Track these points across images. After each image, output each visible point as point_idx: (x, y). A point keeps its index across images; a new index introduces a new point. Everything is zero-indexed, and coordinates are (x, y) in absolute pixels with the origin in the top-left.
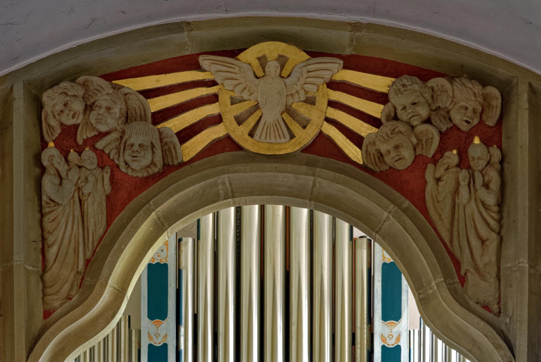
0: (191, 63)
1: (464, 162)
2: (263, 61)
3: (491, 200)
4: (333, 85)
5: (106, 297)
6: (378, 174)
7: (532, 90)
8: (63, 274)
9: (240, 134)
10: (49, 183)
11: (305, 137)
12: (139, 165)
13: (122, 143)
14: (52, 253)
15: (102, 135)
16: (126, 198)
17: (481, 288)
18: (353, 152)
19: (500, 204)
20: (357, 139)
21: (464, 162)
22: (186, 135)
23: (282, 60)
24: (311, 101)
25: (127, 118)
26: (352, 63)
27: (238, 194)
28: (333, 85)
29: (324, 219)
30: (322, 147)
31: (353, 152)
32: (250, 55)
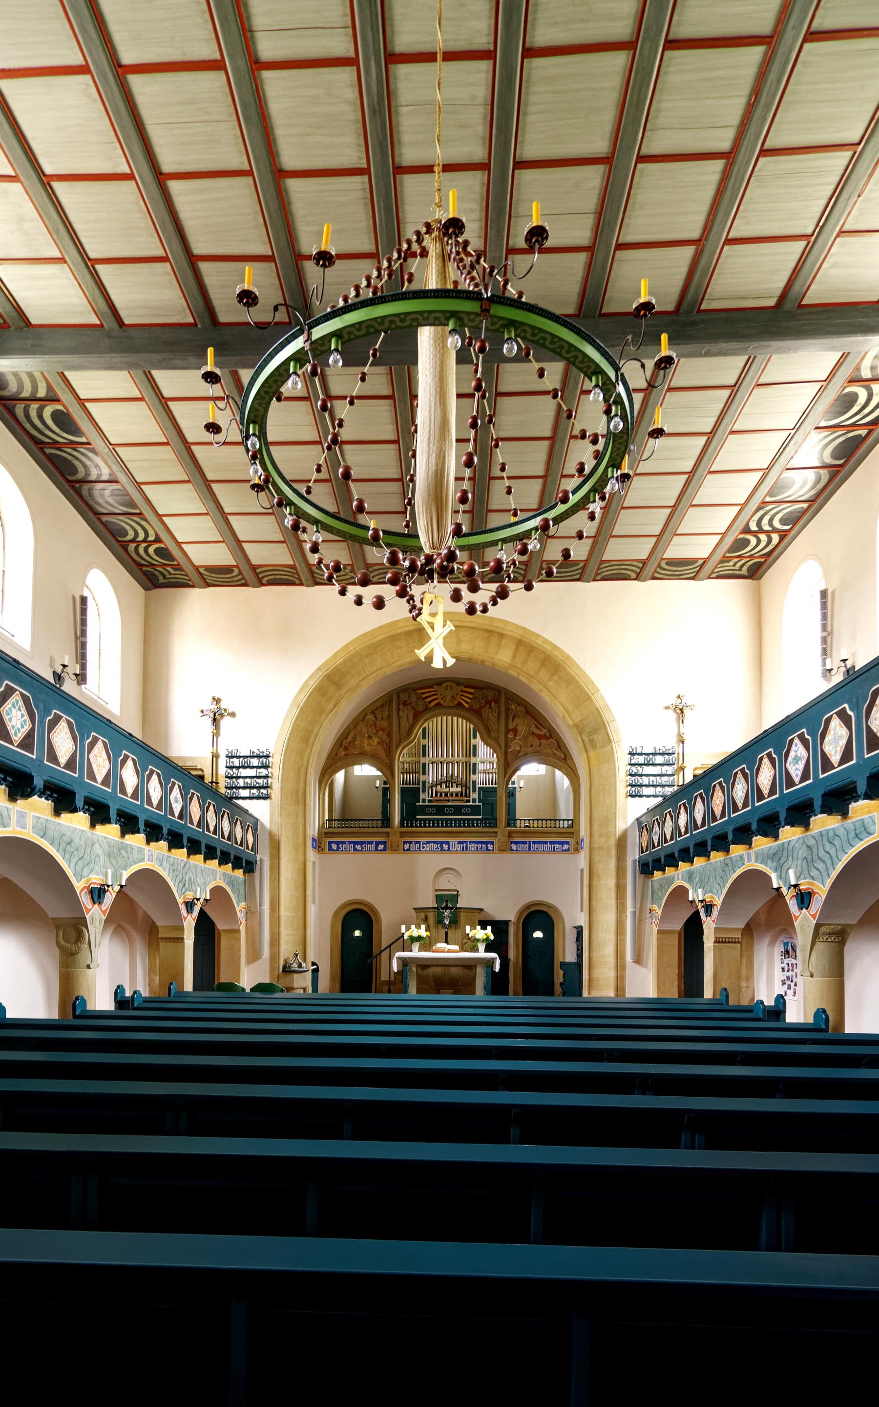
0: (431, 687)
1: (490, 707)
4: (462, 691)
6: (471, 710)
7: (506, 694)
8: (404, 731)
9: (442, 702)
10: (401, 713)
11: (456, 702)
12: (421, 708)
13: (417, 705)
16: (417, 716)
17: (494, 734)
18: (466, 705)
20: (467, 702)
21: (490, 707)
22: (430, 702)
25: (418, 698)
27: (442, 715)
28: (462, 691)
29: (460, 719)
30: (460, 704)
31: (466, 705)
32: (444, 685)
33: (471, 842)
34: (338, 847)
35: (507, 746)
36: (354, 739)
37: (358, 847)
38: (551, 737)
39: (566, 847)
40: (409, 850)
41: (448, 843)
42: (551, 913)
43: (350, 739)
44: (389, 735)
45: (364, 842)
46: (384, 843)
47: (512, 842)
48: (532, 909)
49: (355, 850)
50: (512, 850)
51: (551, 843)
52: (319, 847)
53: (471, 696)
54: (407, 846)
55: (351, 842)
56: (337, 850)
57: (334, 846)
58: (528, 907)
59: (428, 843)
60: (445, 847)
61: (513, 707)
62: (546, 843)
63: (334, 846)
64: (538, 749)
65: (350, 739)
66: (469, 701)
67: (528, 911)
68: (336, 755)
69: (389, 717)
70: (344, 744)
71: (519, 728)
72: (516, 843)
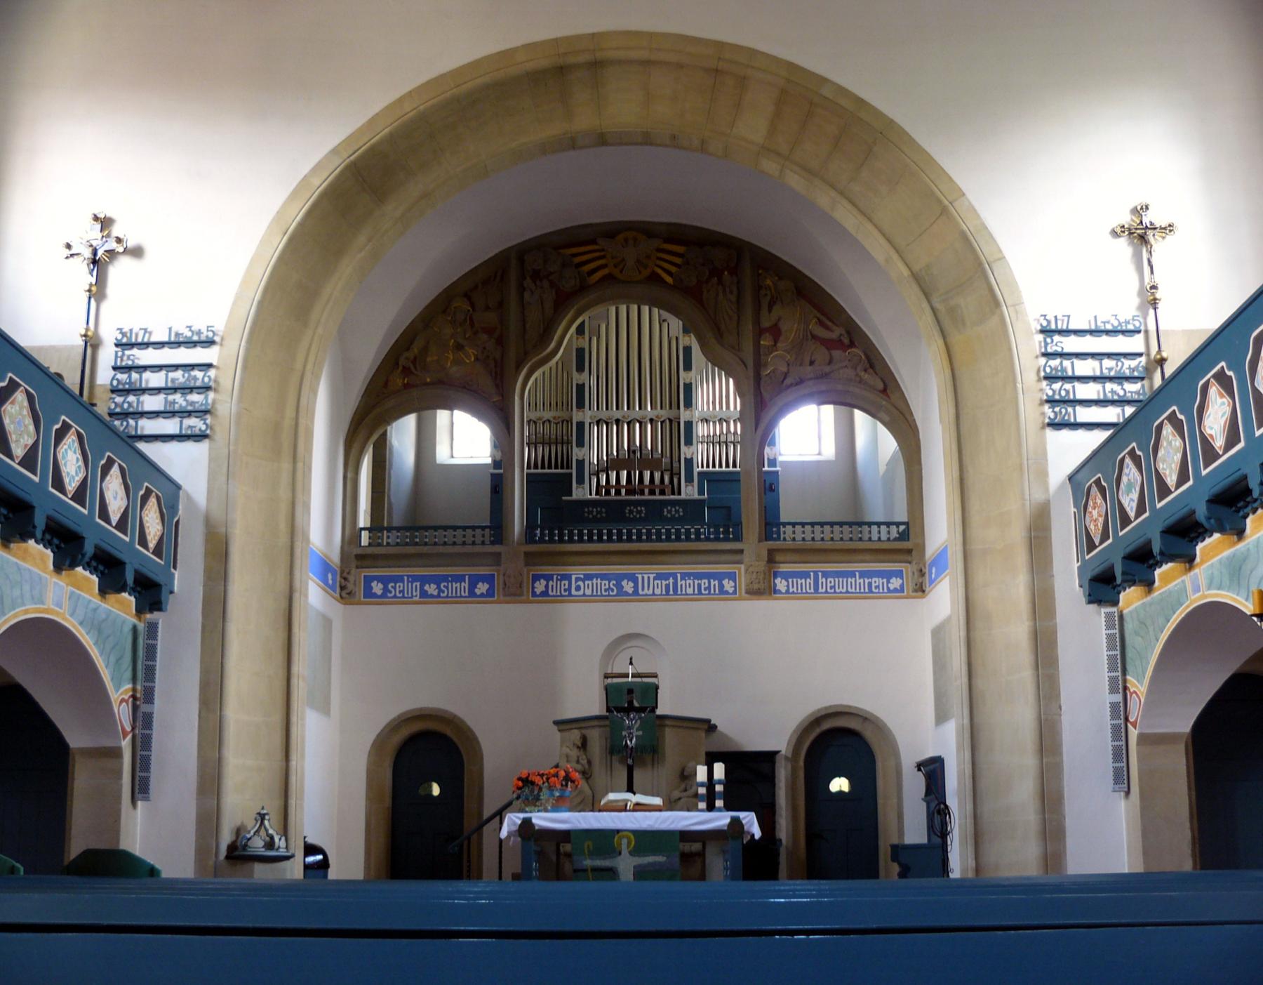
0: (594, 242)
1: (720, 282)
2: (626, 240)
3: (733, 298)
4: (659, 250)
5: (553, 345)
10: (527, 295)
11: (646, 273)
14: (528, 326)
15: (551, 273)
16: (563, 301)
18: (669, 280)
19: (738, 302)
21: (720, 282)
23: (635, 239)
24: (648, 257)
26: (668, 240)
28: (659, 250)
29: (656, 311)
31: (669, 280)
32: (620, 237)
33: (684, 576)
34: (386, 590)
35: (758, 366)
36: (425, 350)
37: (431, 589)
38: (852, 344)
39: (895, 583)
40: (545, 593)
41: (633, 578)
42: (869, 734)
43: (415, 350)
44: (500, 342)
45: (445, 578)
46: (489, 579)
47: (776, 575)
48: (826, 726)
49: (424, 594)
50: (776, 591)
51: (863, 574)
52: (342, 588)
53: (678, 261)
54: (540, 586)
55: (414, 578)
56: (384, 595)
57: (377, 588)
58: (817, 720)
59: (588, 577)
60: (628, 586)
61: (769, 282)
62: (852, 574)
63: (377, 588)
64: (827, 369)
65: (415, 350)
66: (673, 269)
67: (818, 731)
68: (386, 384)
69: (501, 304)
70: (402, 361)
71: (784, 327)
72: (786, 576)
